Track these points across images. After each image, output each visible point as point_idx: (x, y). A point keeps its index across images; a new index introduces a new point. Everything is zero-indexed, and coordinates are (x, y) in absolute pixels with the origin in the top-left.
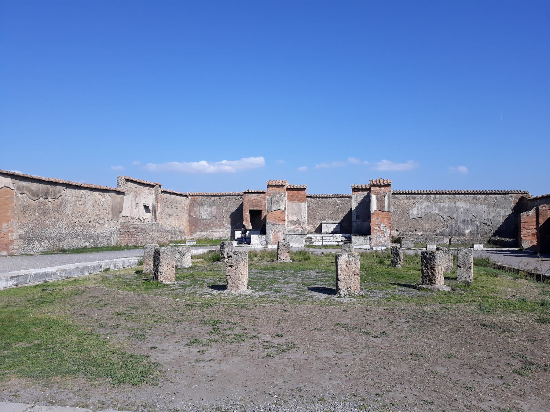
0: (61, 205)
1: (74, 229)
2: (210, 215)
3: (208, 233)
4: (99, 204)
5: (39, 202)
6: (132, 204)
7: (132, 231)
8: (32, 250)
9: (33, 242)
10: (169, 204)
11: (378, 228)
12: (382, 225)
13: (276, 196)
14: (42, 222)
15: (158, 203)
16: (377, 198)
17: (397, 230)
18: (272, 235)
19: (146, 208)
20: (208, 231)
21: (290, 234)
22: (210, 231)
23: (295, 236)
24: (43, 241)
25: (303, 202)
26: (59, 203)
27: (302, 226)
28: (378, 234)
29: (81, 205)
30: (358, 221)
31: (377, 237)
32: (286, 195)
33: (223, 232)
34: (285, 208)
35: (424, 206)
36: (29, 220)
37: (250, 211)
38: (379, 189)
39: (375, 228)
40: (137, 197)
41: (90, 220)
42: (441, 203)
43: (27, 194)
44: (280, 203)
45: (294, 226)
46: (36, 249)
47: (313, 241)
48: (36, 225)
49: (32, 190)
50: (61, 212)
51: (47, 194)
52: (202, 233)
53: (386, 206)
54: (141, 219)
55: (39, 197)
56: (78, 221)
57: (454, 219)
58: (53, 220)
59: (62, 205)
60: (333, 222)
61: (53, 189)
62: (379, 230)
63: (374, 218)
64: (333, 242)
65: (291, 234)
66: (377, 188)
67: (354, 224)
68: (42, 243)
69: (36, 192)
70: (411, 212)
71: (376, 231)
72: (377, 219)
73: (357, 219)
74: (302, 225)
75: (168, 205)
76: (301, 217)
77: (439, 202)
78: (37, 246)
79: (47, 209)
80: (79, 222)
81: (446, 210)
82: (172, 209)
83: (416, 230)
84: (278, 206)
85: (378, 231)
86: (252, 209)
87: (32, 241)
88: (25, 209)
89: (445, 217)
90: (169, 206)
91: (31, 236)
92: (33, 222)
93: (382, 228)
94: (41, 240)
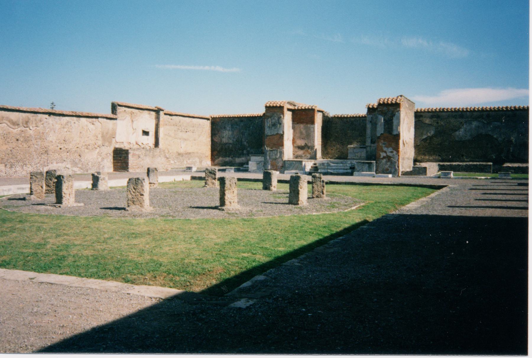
0: (43, 133)
1: (59, 155)
4: (87, 131)
5: (20, 131)
7: (124, 157)
8: (14, 174)
9: (15, 167)
10: (183, 128)
14: (24, 149)
18: (271, 161)
19: (146, 133)
24: (26, 166)
26: (41, 132)
29: (66, 132)
30: (373, 145)
36: (10, 147)
38: (386, 109)
40: (135, 123)
41: (78, 146)
43: (7, 124)
44: (278, 127)
46: (19, 173)
47: (319, 168)
48: (17, 151)
49: (12, 120)
50: (43, 139)
51: (28, 123)
54: (140, 144)
55: (19, 126)
56: (64, 147)
58: (36, 146)
59: (45, 133)
61: (34, 118)
63: (381, 142)
64: (341, 169)
66: (385, 108)
68: (25, 167)
69: (16, 122)
75: (182, 129)
78: (19, 171)
79: (28, 137)
80: (64, 149)
82: (188, 133)
87: (14, 165)
88: (5, 137)
90: (184, 130)
91: (12, 161)
92: (13, 148)
94: (23, 165)
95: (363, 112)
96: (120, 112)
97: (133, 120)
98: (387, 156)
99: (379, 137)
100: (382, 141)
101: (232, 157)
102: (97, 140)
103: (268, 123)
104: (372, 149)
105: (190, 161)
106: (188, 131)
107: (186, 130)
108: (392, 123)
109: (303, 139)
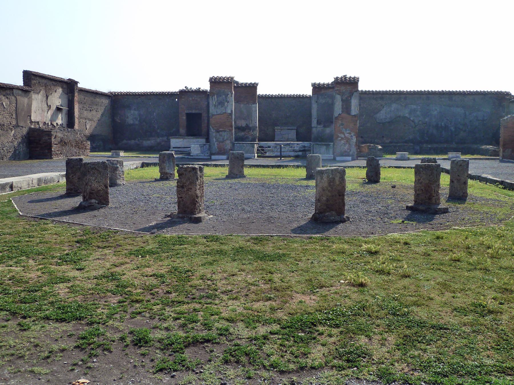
2: (139, 119)
3: (137, 141)
6: (43, 106)
11: (343, 136)
12: (348, 132)
13: (220, 96)
15: (75, 105)
16: (342, 100)
17: (362, 137)
18: (217, 144)
20: (137, 139)
21: (238, 143)
22: (139, 139)
23: (244, 145)
25: (254, 104)
27: (252, 133)
28: (343, 142)
31: (342, 145)
32: (233, 95)
33: (154, 141)
34: (232, 111)
35: (393, 109)
37: (188, 115)
38: (344, 88)
39: (340, 135)
42: (412, 106)
45: (243, 133)
52: (129, 142)
53: (353, 108)
57: (426, 123)
60: (289, 128)
62: (344, 137)
65: (240, 143)
67: (314, 130)
70: (378, 115)
71: (340, 139)
72: (342, 124)
73: (317, 124)
74: (252, 132)
75: (87, 107)
76: (251, 122)
77: (410, 105)
81: (418, 113)
83: (383, 137)
84: (223, 108)
85: (342, 139)
86: (190, 112)
89: (416, 121)
90: (88, 109)
93: (347, 135)
95: (308, 92)
96: (35, 84)
97: (48, 95)
98: (345, 137)
99: (337, 117)
100: (340, 122)
101: (138, 140)
102: (12, 118)
103: (213, 101)
104: (318, 130)
105: (95, 144)
106: (92, 110)
107: (90, 109)
108: (350, 103)
109: (243, 119)
